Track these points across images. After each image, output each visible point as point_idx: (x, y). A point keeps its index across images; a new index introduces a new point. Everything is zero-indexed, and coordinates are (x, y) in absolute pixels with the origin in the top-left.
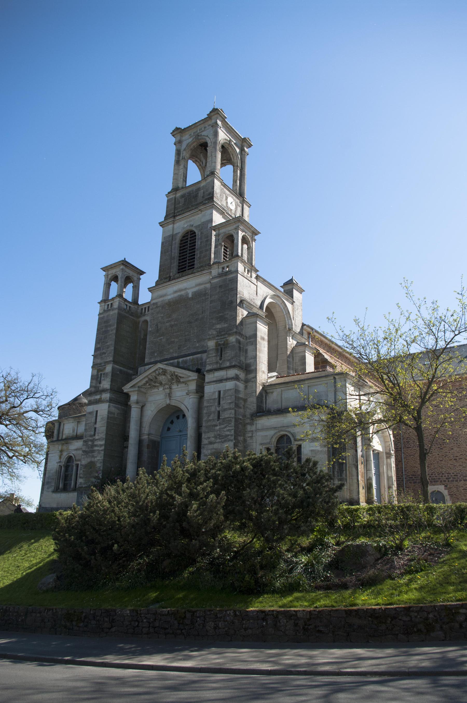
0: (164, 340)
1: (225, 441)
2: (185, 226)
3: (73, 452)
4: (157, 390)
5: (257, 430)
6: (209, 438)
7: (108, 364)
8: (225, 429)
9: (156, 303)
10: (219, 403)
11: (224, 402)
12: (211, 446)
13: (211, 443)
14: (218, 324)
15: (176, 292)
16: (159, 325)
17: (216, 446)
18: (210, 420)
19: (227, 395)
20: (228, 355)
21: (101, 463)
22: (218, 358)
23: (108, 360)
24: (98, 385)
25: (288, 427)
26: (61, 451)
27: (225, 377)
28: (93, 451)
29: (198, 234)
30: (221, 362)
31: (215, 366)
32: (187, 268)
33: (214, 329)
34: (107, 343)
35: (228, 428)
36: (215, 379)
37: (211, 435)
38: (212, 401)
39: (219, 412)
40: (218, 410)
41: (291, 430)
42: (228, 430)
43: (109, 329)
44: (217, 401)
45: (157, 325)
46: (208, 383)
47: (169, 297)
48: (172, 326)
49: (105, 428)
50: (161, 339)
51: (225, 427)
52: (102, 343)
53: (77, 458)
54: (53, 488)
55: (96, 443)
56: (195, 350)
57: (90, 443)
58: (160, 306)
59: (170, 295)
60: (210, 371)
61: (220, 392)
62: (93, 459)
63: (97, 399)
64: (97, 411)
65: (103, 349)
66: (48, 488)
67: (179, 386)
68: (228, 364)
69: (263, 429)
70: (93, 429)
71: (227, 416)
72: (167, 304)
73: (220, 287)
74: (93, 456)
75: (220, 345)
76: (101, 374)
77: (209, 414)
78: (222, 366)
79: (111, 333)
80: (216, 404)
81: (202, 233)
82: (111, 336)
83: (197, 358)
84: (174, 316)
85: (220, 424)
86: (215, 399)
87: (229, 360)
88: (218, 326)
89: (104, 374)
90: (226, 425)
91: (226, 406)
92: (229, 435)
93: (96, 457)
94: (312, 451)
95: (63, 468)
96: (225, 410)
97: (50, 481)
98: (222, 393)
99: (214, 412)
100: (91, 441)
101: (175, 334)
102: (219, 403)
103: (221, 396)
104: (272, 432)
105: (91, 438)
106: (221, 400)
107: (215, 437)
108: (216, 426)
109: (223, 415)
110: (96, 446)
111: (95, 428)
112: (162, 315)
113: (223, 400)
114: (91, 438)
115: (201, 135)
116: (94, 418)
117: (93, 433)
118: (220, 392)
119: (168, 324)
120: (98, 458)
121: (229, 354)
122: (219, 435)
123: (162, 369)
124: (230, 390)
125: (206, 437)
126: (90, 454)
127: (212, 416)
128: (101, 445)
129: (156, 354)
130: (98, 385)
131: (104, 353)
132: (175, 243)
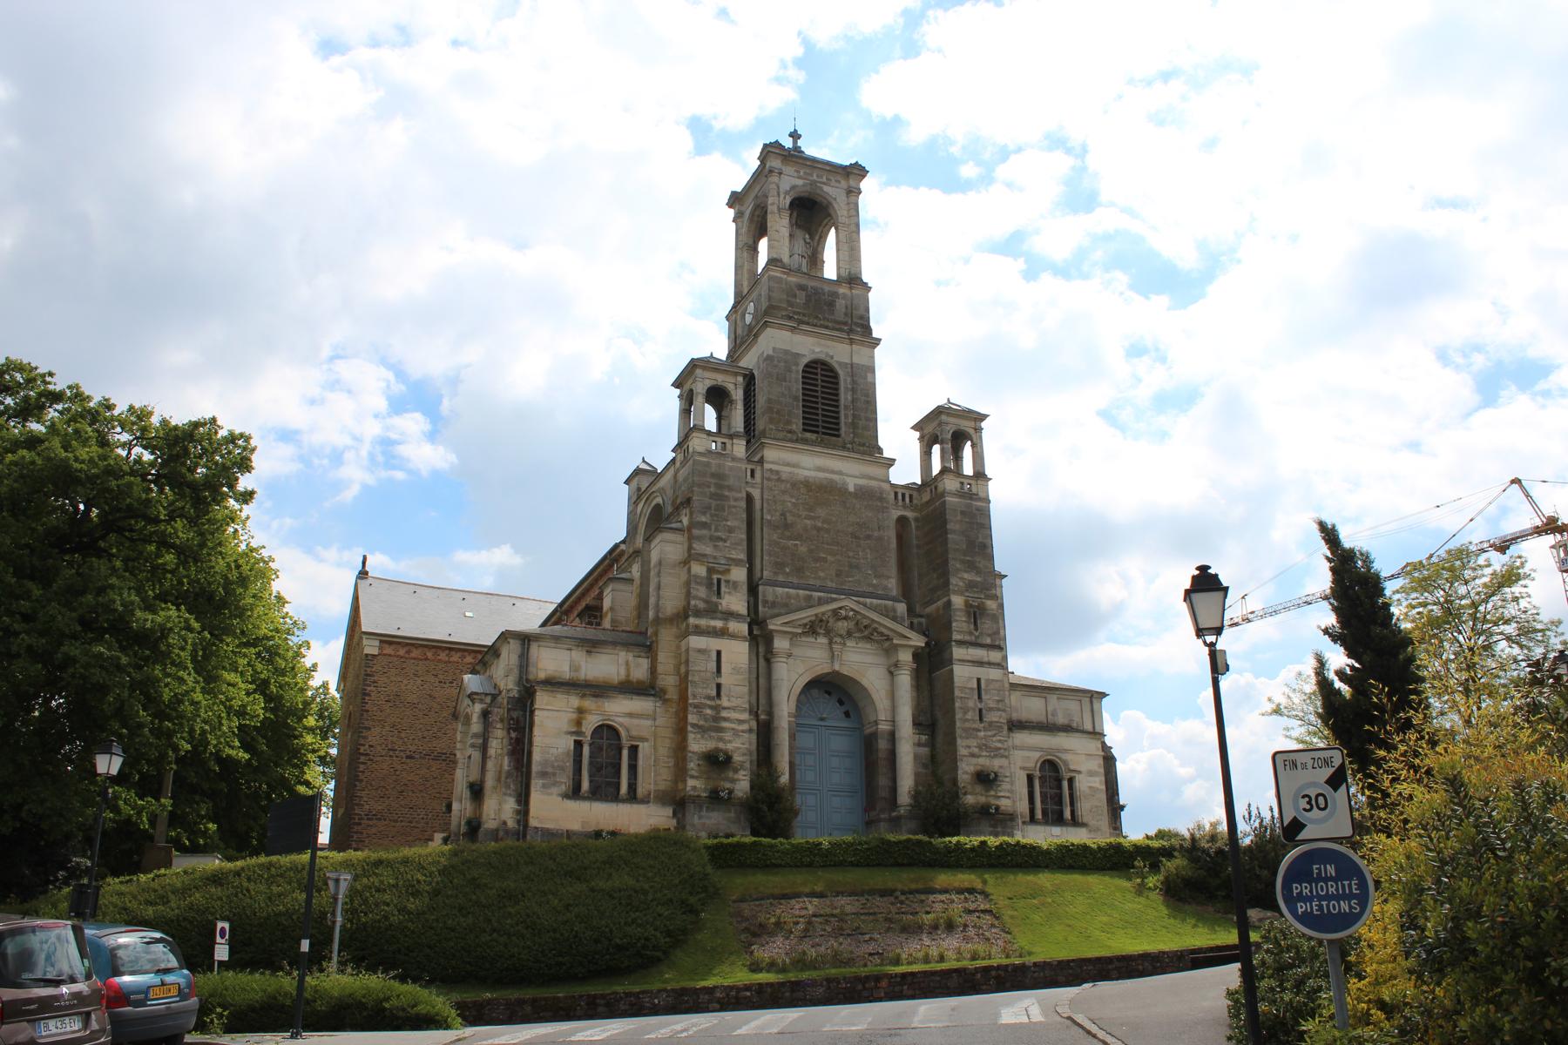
0: (803, 549)
1: (995, 756)
2: (817, 350)
3: (621, 720)
4: (813, 640)
5: (1015, 747)
6: (969, 747)
7: (737, 565)
8: (994, 739)
9: (777, 472)
10: (980, 697)
11: (988, 697)
12: (974, 760)
13: (973, 755)
14: (966, 572)
15: (819, 469)
16: (790, 518)
17: (981, 761)
18: (967, 720)
19: (992, 687)
20: (987, 626)
21: (744, 755)
22: (972, 626)
23: (734, 557)
24: (714, 599)
25: (1059, 751)
26: (581, 711)
27: (986, 659)
28: (721, 730)
29: (845, 380)
30: (977, 634)
31: (967, 638)
32: (820, 429)
33: (960, 578)
34: (727, 520)
35: (999, 738)
36: (969, 658)
37: (973, 743)
38: (967, 691)
39: (980, 710)
40: (979, 706)
41: (1063, 756)
42: (1000, 741)
43: (727, 493)
44: (976, 692)
45: (783, 514)
46: (959, 660)
47: (807, 473)
48: (819, 529)
49: (746, 690)
50: (796, 545)
51: (994, 736)
52: (712, 516)
53: (634, 733)
54: (563, 787)
55: (724, 714)
56: (871, 589)
57: (709, 711)
58: (787, 481)
59: (810, 470)
60: (961, 643)
61: (979, 680)
62: (721, 745)
63: (715, 627)
64: (719, 653)
65: (716, 530)
66: (544, 786)
67: (860, 645)
68: (988, 641)
69: (1022, 748)
70: (715, 686)
71: (994, 719)
72: (802, 483)
73: (962, 513)
74: (721, 739)
75: (971, 606)
76: (719, 581)
77: (966, 711)
78: (979, 641)
79: (732, 503)
80: (976, 697)
81: (854, 382)
82: (734, 510)
83: (886, 606)
84: (821, 512)
85: (985, 729)
86: (972, 689)
87: (989, 635)
88: (966, 576)
89: (727, 582)
90: (993, 732)
91: (992, 705)
92: (1000, 749)
93: (730, 742)
94: (1090, 787)
95: (586, 750)
96: (991, 709)
97: (550, 770)
98: (983, 682)
99: (974, 709)
100: (711, 707)
101: (826, 546)
102: (980, 697)
103: (983, 686)
104: (1037, 755)
105: (709, 702)
106: (983, 693)
107: (979, 747)
108: (980, 731)
109: (989, 717)
110: (726, 719)
111: (719, 686)
112: (794, 500)
113: (986, 694)
114: (709, 702)
115: (821, 189)
116: (715, 664)
117: (714, 693)
118: (979, 680)
119: (808, 522)
120: (734, 745)
121: (986, 625)
122: (985, 745)
123: (852, 610)
124: (997, 681)
125: (964, 744)
126: (713, 734)
127: (970, 713)
128: (741, 722)
129: (788, 570)
130: (714, 599)
131: (720, 539)
132: (797, 371)
